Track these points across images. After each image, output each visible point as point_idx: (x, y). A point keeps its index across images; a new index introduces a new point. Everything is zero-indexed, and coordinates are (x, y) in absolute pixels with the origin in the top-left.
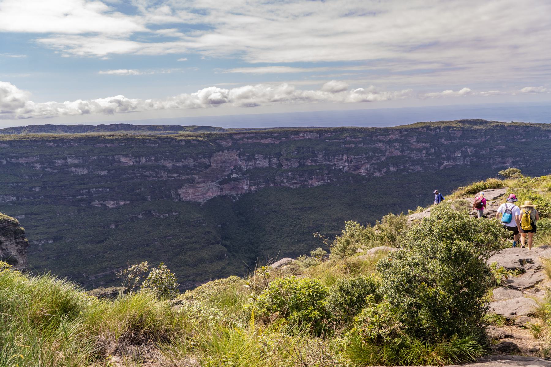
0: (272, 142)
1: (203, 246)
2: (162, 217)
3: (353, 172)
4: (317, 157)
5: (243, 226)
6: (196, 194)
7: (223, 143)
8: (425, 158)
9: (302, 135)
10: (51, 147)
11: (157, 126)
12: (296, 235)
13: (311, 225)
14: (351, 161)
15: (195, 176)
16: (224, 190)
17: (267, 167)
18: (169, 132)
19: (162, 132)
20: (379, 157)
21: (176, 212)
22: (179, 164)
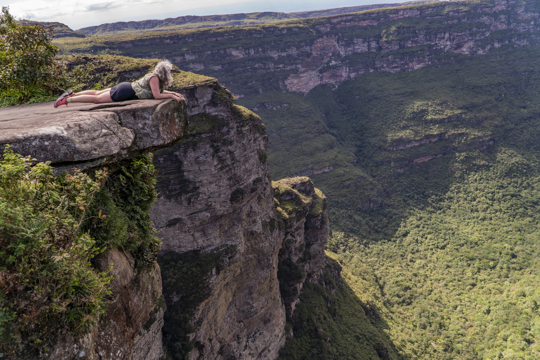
0: (370, 24)
2: (275, 109)
3: (455, 52)
4: (418, 37)
5: (345, 114)
6: (300, 84)
7: (322, 29)
8: (532, 31)
9: (401, 13)
11: (221, 16)
12: (400, 121)
13: (415, 110)
14: (454, 39)
15: (299, 66)
17: (366, 52)
18: (234, 21)
19: (228, 22)
21: (286, 104)
22: (284, 54)
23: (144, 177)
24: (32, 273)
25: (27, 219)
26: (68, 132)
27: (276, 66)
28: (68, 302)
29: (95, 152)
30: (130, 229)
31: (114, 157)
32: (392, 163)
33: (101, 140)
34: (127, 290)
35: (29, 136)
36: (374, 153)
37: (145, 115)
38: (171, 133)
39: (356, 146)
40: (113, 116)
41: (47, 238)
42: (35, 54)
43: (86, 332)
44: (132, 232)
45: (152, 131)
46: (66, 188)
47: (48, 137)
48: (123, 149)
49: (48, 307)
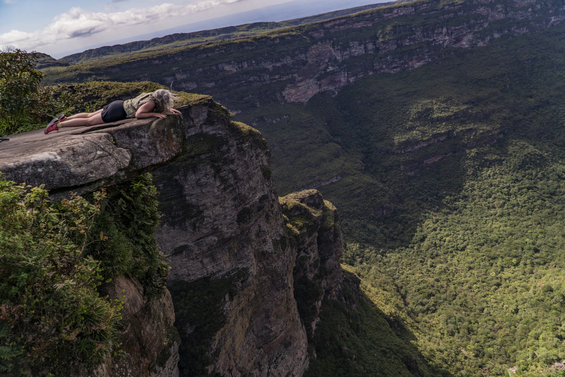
1: (319, 146)
2: (274, 122)
3: (454, 46)
4: (415, 34)
6: (298, 94)
7: (316, 35)
9: (395, 11)
10: (157, 65)
11: (209, 31)
12: (406, 122)
13: (420, 110)
14: (452, 33)
15: (296, 75)
16: (322, 86)
17: (363, 54)
18: (224, 35)
19: (217, 36)
20: (482, 23)
21: (286, 115)
22: (279, 64)
23: (144, 200)
24: (37, 304)
25: (27, 248)
26: (61, 156)
27: (272, 77)
28: (77, 331)
29: (91, 175)
30: (136, 254)
31: (112, 180)
32: (402, 167)
33: (97, 162)
34: (138, 319)
35: (21, 164)
36: (382, 158)
37: (141, 133)
38: (169, 150)
39: (363, 152)
40: (107, 137)
41: (50, 266)
42: (19, 81)
43: (100, 362)
44: (138, 257)
45: (149, 149)
46: (64, 215)
47: (41, 164)
48: (120, 170)
49: (57, 338)
